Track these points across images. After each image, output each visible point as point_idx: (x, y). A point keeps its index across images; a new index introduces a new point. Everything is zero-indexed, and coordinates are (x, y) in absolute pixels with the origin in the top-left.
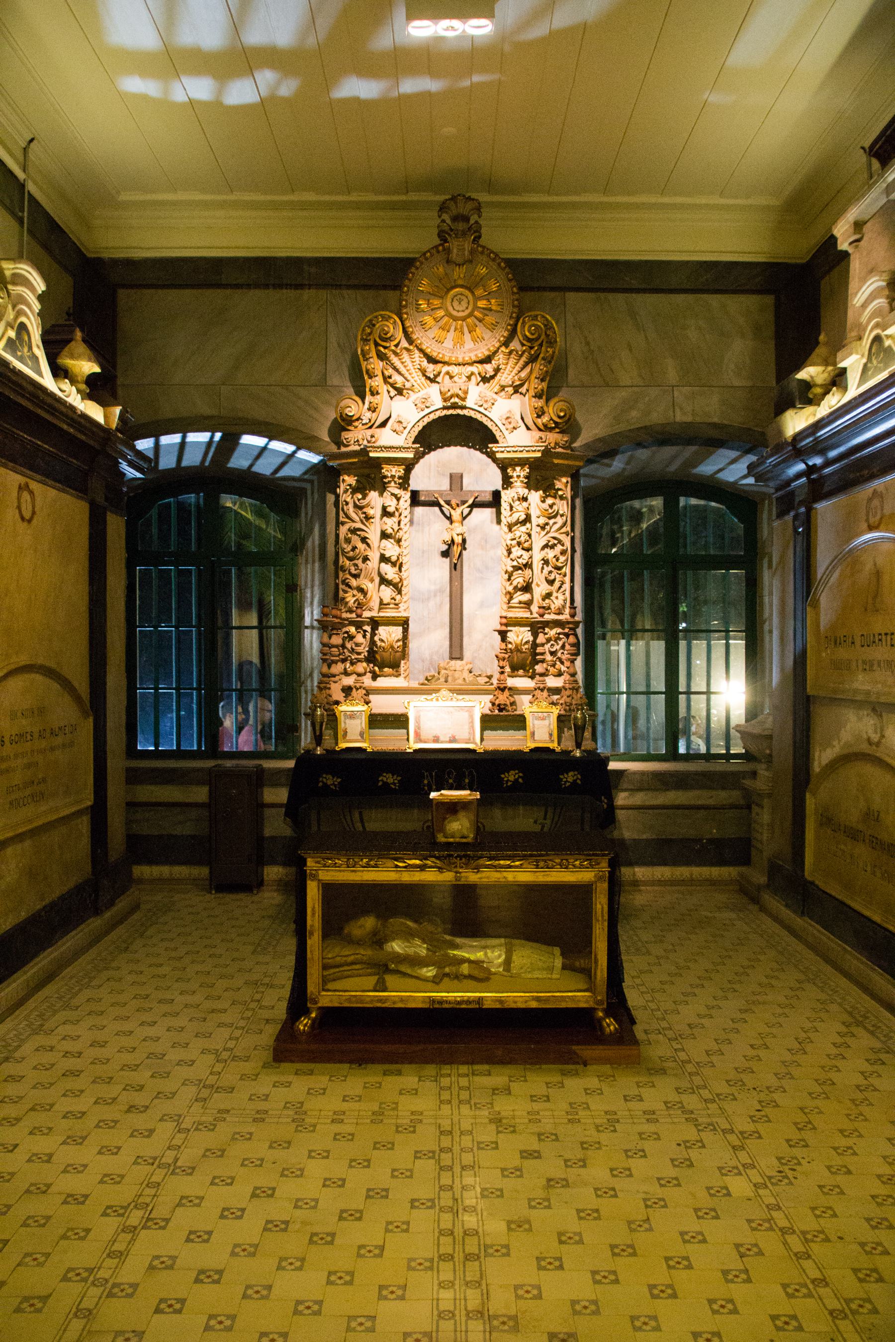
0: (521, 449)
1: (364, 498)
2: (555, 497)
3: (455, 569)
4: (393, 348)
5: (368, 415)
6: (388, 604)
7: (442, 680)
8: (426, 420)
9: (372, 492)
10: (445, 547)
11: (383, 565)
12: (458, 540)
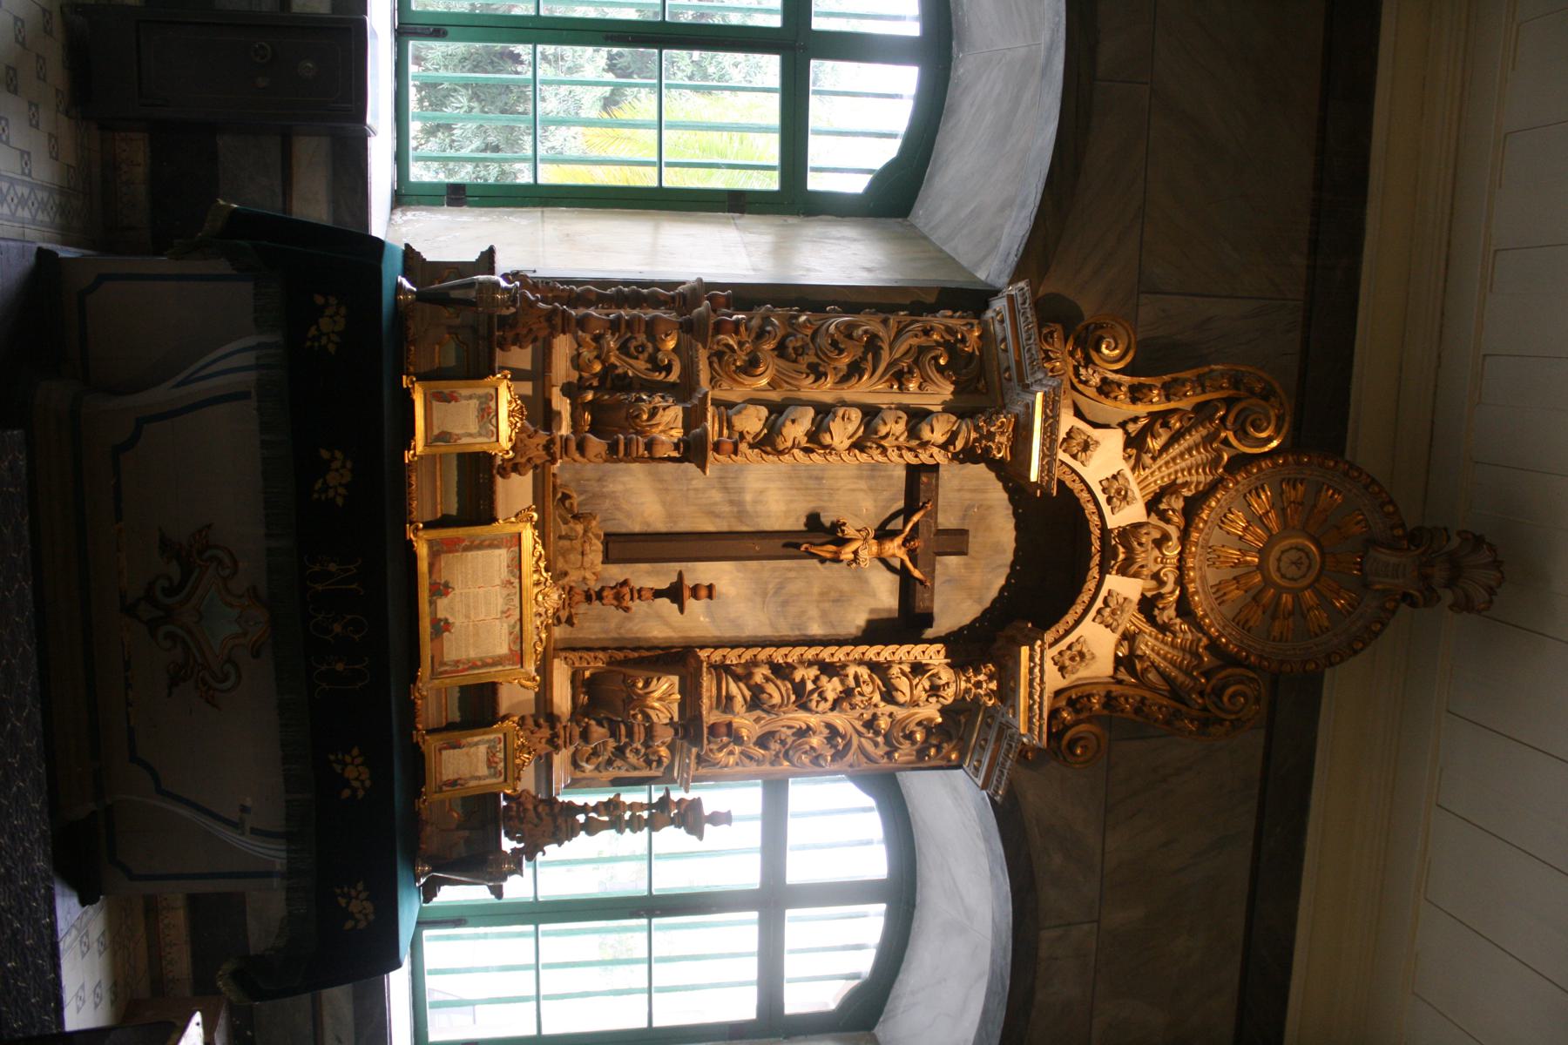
0: (1036, 697)
1: (941, 370)
2: (926, 741)
3: (786, 545)
4: (1223, 435)
5: (1096, 380)
6: (730, 426)
7: (564, 529)
8: (1085, 496)
9: (951, 388)
10: (827, 520)
11: (811, 412)
12: (847, 553)
